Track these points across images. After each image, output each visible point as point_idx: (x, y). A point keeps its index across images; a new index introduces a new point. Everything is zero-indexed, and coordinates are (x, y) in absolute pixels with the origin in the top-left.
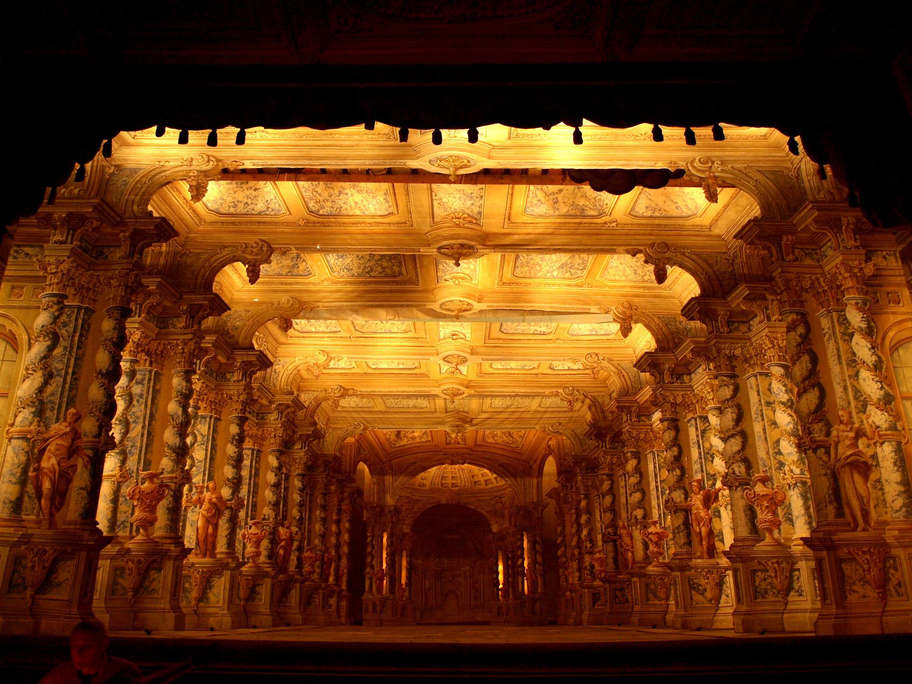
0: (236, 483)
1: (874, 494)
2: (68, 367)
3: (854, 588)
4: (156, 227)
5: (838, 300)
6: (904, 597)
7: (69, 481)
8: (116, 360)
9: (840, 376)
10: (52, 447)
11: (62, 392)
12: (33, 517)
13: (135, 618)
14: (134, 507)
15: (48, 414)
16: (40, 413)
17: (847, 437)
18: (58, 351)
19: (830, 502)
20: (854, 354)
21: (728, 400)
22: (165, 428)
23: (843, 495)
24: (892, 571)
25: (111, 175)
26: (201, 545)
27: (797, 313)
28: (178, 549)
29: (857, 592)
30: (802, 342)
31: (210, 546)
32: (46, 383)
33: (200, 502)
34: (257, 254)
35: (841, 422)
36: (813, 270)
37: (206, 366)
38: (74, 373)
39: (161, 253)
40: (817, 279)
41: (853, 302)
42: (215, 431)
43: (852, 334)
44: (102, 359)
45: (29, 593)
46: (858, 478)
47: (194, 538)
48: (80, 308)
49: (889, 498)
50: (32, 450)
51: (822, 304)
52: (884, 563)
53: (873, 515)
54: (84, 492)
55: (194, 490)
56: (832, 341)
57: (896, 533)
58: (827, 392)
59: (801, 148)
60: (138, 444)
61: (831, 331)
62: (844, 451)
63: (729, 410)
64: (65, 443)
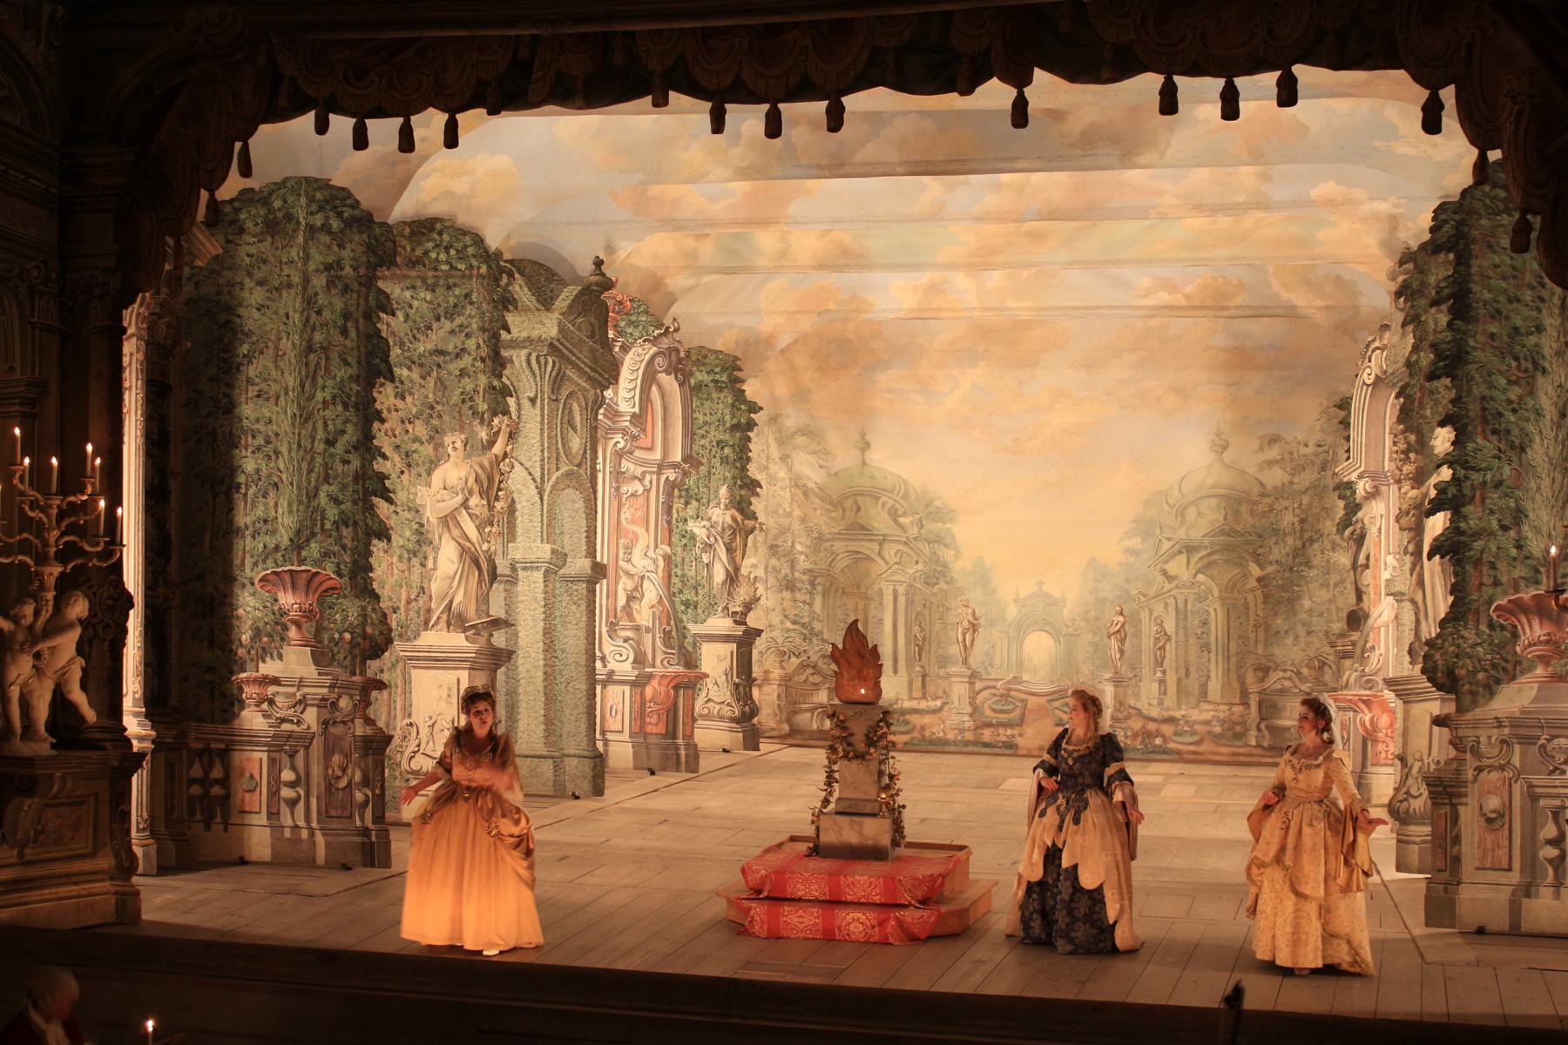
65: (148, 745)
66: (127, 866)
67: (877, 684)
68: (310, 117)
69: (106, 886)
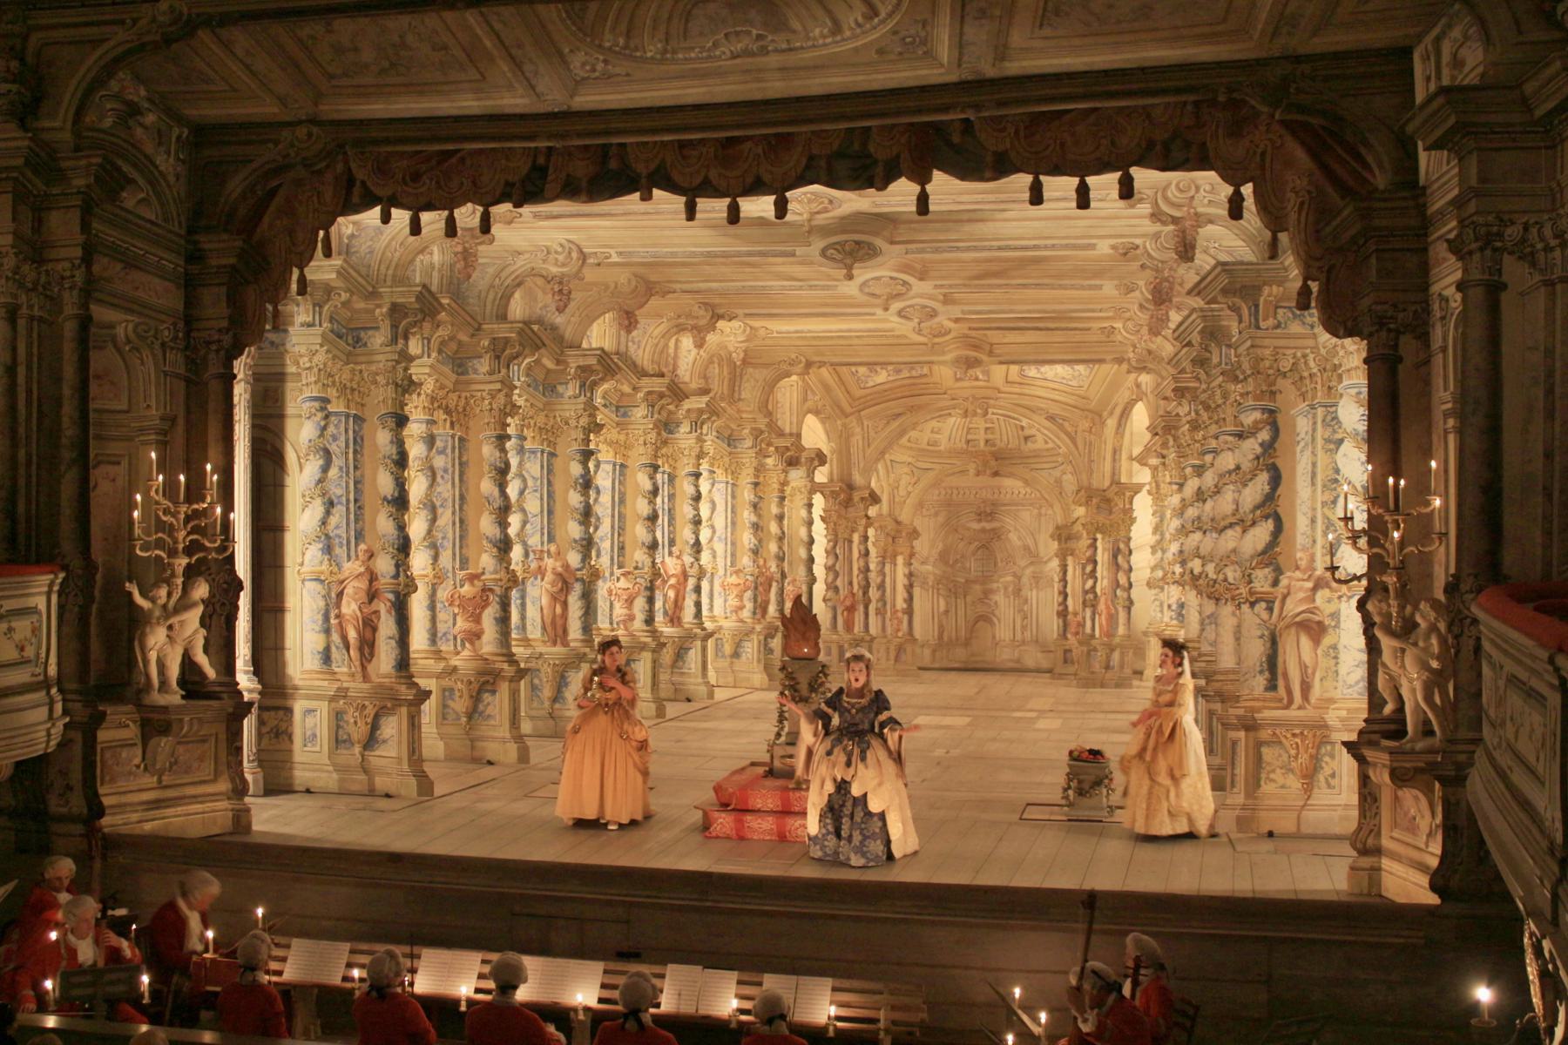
0: (587, 545)
1: (1324, 663)
2: (348, 493)
3: (1272, 776)
4: (418, 298)
5: (1330, 388)
6: (1336, 791)
7: (375, 630)
8: (401, 484)
9: (1309, 503)
10: (349, 591)
11: (348, 524)
12: (345, 670)
13: (473, 748)
14: (455, 615)
15: (338, 550)
16: (328, 550)
17: (1301, 589)
18: (333, 472)
19: (1261, 672)
20: (1337, 471)
21: (1230, 472)
22: (481, 513)
23: (1280, 659)
24: (1327, 759)
25: (352, 236)
26: (549, 629)
27: (1264, 410)
28: (513, 669)
29: (1273, 781)
30: (1263, 454)
31: (560, 632)
32: (328, 513)
33: (541, 572)
34: (563, 265)
35: (1298, 568)
36: (1299, 343)
37: (528, 375)
38: (356, 501)
39: (432, 266)
40: (1305, 356)
41: (1353, 391)
42: (550, 471)
43: (1341, 441)
44: (385, 483)
45: (357, 749)
46: (1305, 642)
47: (539, 620)
48: (347, 416)
49: (1343, 669)
50: (329, 594)
51: (1303, 396)
52: (1319, 748)
53: (1316, 692)
54: (393, 643)
55: (532, 556)
56: (1308, 453)
57: (1344, 713)
58: (1286, 526)
59: (1249, 203)
60: (450, 535)
61: (1309, 438)
62: (1293, 607)
63: (1231, 487)
64: (363, 584)
65: (256, 696)
66: (240, 790)
67: (817, 644)
68: (377, 211)
69: (224, 804)
